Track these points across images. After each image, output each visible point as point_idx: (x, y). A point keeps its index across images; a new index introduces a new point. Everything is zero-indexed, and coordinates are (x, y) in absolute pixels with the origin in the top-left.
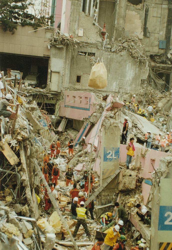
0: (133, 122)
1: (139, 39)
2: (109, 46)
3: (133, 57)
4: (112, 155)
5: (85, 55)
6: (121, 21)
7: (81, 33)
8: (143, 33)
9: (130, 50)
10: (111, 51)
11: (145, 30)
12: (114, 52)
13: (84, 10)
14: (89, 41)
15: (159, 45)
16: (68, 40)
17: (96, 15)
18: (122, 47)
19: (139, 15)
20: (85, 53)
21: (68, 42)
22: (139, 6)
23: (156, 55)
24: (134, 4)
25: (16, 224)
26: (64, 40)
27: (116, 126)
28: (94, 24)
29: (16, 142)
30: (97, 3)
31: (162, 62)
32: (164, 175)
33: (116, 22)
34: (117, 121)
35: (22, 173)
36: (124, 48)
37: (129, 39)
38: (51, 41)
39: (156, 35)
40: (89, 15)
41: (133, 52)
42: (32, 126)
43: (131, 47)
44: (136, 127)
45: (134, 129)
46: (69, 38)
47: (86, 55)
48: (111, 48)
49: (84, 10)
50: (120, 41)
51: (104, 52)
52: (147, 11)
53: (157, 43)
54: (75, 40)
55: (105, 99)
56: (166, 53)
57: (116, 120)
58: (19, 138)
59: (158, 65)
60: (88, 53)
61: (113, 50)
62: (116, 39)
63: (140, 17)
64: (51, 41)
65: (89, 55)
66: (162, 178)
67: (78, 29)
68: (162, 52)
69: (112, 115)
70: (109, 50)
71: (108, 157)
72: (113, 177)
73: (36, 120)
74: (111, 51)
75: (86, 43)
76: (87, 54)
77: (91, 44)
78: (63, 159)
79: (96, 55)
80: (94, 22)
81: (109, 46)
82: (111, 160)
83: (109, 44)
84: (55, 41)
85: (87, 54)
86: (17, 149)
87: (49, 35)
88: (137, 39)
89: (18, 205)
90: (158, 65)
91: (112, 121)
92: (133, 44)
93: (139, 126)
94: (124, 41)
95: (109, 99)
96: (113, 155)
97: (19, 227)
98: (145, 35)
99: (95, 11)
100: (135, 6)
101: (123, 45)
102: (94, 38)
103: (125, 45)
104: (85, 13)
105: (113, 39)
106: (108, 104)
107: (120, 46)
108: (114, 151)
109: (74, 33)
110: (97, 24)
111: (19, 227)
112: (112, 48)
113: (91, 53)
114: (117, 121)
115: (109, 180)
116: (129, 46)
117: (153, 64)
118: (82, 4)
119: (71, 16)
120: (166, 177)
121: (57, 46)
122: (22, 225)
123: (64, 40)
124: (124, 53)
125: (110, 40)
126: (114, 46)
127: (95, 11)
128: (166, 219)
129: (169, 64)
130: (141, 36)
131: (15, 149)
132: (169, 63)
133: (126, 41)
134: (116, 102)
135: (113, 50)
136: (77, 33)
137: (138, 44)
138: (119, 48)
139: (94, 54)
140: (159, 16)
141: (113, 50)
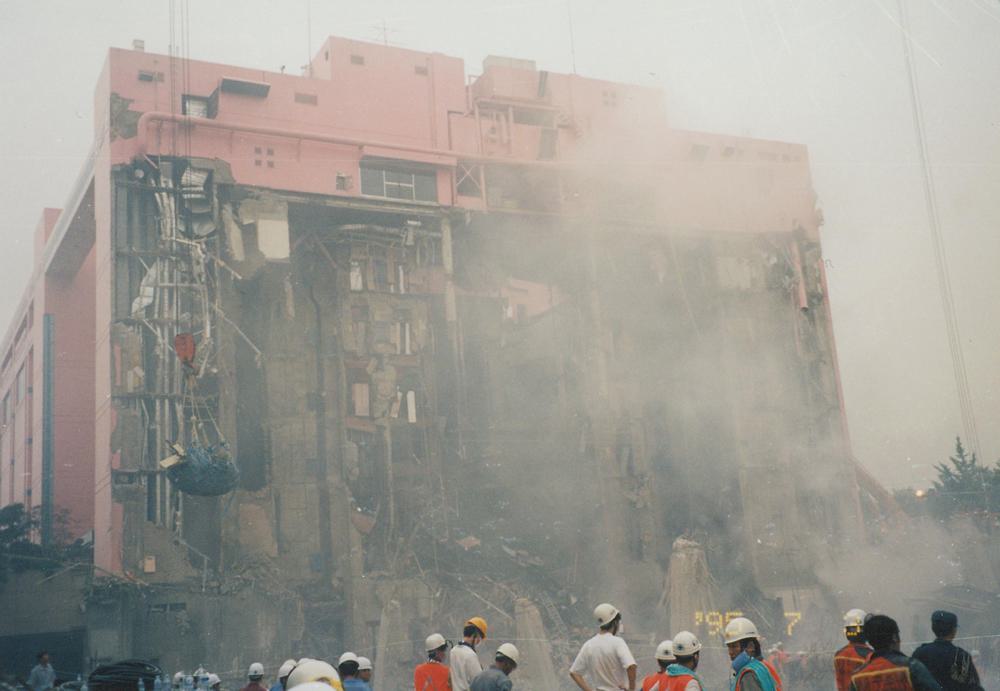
1: (270, 557)
2: (215, 584)
5: (162, 610)
7: (150, 565)
8: (276, 546)
9: (261, 585)
10: (219, 593)
12: (227, 593)
13: (150, 518)
16: (124, 585)
17: (178, 523)
18: (242, 581)
20: (164, 606)
24: (249, 490)
26: (116, 587)
28: (177, 543)
30: (178, 499)
33: (223, 531)
36: (247, 583)
37: (255, 563)
40: (164, 524)
43: (261, 577)
47: (165, 610)
48: (219, 587)
49: (151, 517)
50: (235, 568)
60: (171, 606)
61: (224, 592)
65: (171, 609)
70: (216, 591)
74: (219, 593)
75: (164, 585)
76: (168, 607)
79: (188, 607)
80: (176, 538)
81: (215, 584)
83: (213, 580)
84: (97, 591)
85: (168, 607)
87: (80, 583)
92: (263, 570)
99: (175, 516)
101: (244, 576)
103: (248, 574)
104: (155, 523)
107: (238, 579)
109: (136, 567)
110: (183, 542)
112: (222, 587)
113: (176, 605)
116: (257, 577)
121: (103, 603)
123: (118, 586)
125: (216, 570)
126: (224, 581)
127: (175, 516)
130: (274, 553)
132: (338, 597)
133: (250, 567)
136: (140, 566)
138: (237, 583)
139: (183, 606)
141: (224, 589)
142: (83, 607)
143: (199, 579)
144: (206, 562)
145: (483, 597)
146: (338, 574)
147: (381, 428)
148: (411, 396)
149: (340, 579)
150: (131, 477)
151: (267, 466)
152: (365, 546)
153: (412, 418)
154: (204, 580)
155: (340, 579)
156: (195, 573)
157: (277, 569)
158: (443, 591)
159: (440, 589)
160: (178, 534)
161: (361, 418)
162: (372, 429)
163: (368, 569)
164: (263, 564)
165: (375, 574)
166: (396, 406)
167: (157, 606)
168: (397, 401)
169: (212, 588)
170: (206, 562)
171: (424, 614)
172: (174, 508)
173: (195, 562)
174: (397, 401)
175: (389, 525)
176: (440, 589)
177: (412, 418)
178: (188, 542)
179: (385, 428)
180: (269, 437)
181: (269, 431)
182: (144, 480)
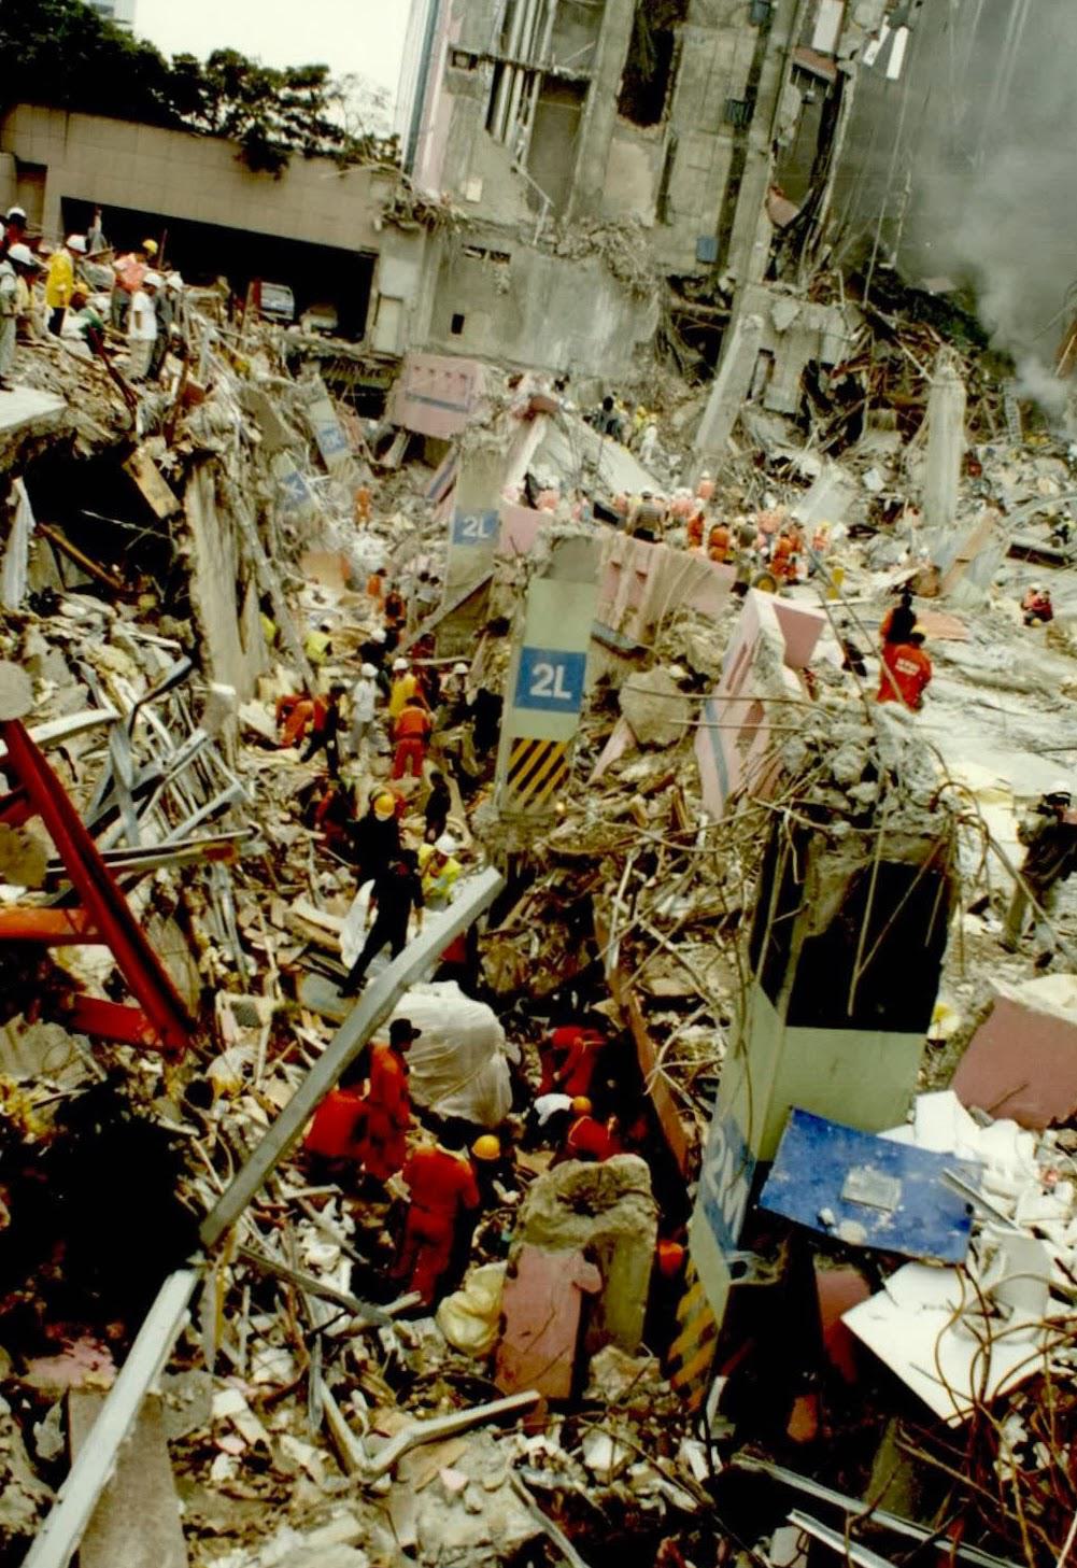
0: (585, 457)
2: (552, 238)
3: (616, 276)
4: (476, 529)
6: (595, 170)
7: (474, 191)
8: (654, 211)
9: (611, 256)
11: (662, 202)
12: (564, 256)
13: (489, 125)
14: (496, 218)
15: (697, 251)
16: (433, 207)
17: (522, 143)
19: (646, 159)
20: (483, 251)
21: (434, 215)
22: (653, 131)
23: (688, 279)
25: (127, 650)
26: (421, 207)
27: (492, 453)
28: (514, 170)
29: (174, 458)
30: (528, 109)
31: (703, 300)
32: (541, 570)
33: (578, 169)
34: (498, 439)
35: (183, 538)
36: (594, 247)
38: (387, 207)
39: (694, 222)
41: (619, 261)
42: (261, 432)
44: (591, 472)
45: (586, 477)
46: (437, 201)
49: (489, 125)
50: (586, 225)
51: (535, 252)
52: (672, 149)
53: (692, 244)
54: (455, 210)
55: (514, 384)
56: (716, 274)
57: (495, 434)
58: (186, 447)
59: (690, 306)
61: (561, 251)
62: (574, 220)
63: (651, 166)
64: (387, 207)
66: (534, 577)
67: (467, 179)
68: (705, 270)
69: (487, 420)
70: (552, 248)
71: (467, 532)
72: (473, 587)
73: (281, 418)
75: (488, 222)
76: (487, 255)
77: (500, 226)
78: (381, 542)
79: (512, 259)
81: (552, 238)
82: (473, 541)
83: (552, 232)
84: (399, 208)
85: (487, 255)
86: (178, 476)
87: (381, 191)
88: (636, 226)
89: (167, 619)
90: (690, 306)
91: (485, 436)
92: (619, 237)
93: (603, 470)
94: (596, 226)
95: (526, 386)
96: (481, 529)
97: (135, 659)
98: (661, 215)
99: (521, 130)
100: (640, 129)
102: (510, 210)
103: (598, 238)
105: (565, 219)
106: (520, 399)
108: (482, 521)
109: (456, 190)
110: (522, 170)
111: (135, 659)
114: (498, 439)
115: (464, 594)
117: (676, 302)
118: (485, 109)
119: (450, 138)
120: (546, 575)
121: (403, 224)
122: (146, 655)
124: (592, 262)
125: (558, 220)
128: (535, 680)
129: (718, 306)
130: (650, 219)
131: (172, 476)
132: (722, 303)
133: (603, 229)
134: (540, 397)
135: (562, 249)
136: (462, 190)
137: (635, 241)
139: (506, 257)
140: (705, 165)
142: (378, 225)
143: (533, 226)
144: (546, 207)
145: (918, 358)
146: (731, 273)
147: (842, 77)
148: (902, 35)
149: (732, 281)
150: (473, 61)
151: (667, 95)
152: (776, 243)
153: (894, 70)
154: (539, 229)
155: (732, 281)
156: (528, 216)
157: (643, 242)
158: (863, 335)
159: (861, 331)
160: (519, 159)
161: (816, 51)
162: (831, 76)
163: (771, 275)
164: (622, 230)
165: (779, 284)
166: (875, 47)
167: (472, 248)
168: (877, 38)
169: (547, 243)
170: (546, 207)
171: (827, 358)
172: (521, 120)
173: (534, 204)
174: (877, 38)
175: (816, 222)
176: (861, 331)
177: (894, 70)
178: (530, 172)
179: (849, 77)
180: (680, 51)
181: (682, 44)
182: (487, 72)
